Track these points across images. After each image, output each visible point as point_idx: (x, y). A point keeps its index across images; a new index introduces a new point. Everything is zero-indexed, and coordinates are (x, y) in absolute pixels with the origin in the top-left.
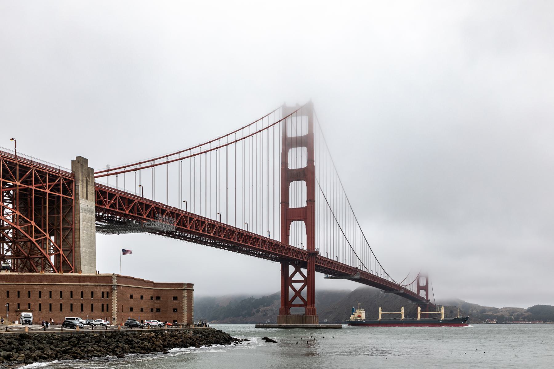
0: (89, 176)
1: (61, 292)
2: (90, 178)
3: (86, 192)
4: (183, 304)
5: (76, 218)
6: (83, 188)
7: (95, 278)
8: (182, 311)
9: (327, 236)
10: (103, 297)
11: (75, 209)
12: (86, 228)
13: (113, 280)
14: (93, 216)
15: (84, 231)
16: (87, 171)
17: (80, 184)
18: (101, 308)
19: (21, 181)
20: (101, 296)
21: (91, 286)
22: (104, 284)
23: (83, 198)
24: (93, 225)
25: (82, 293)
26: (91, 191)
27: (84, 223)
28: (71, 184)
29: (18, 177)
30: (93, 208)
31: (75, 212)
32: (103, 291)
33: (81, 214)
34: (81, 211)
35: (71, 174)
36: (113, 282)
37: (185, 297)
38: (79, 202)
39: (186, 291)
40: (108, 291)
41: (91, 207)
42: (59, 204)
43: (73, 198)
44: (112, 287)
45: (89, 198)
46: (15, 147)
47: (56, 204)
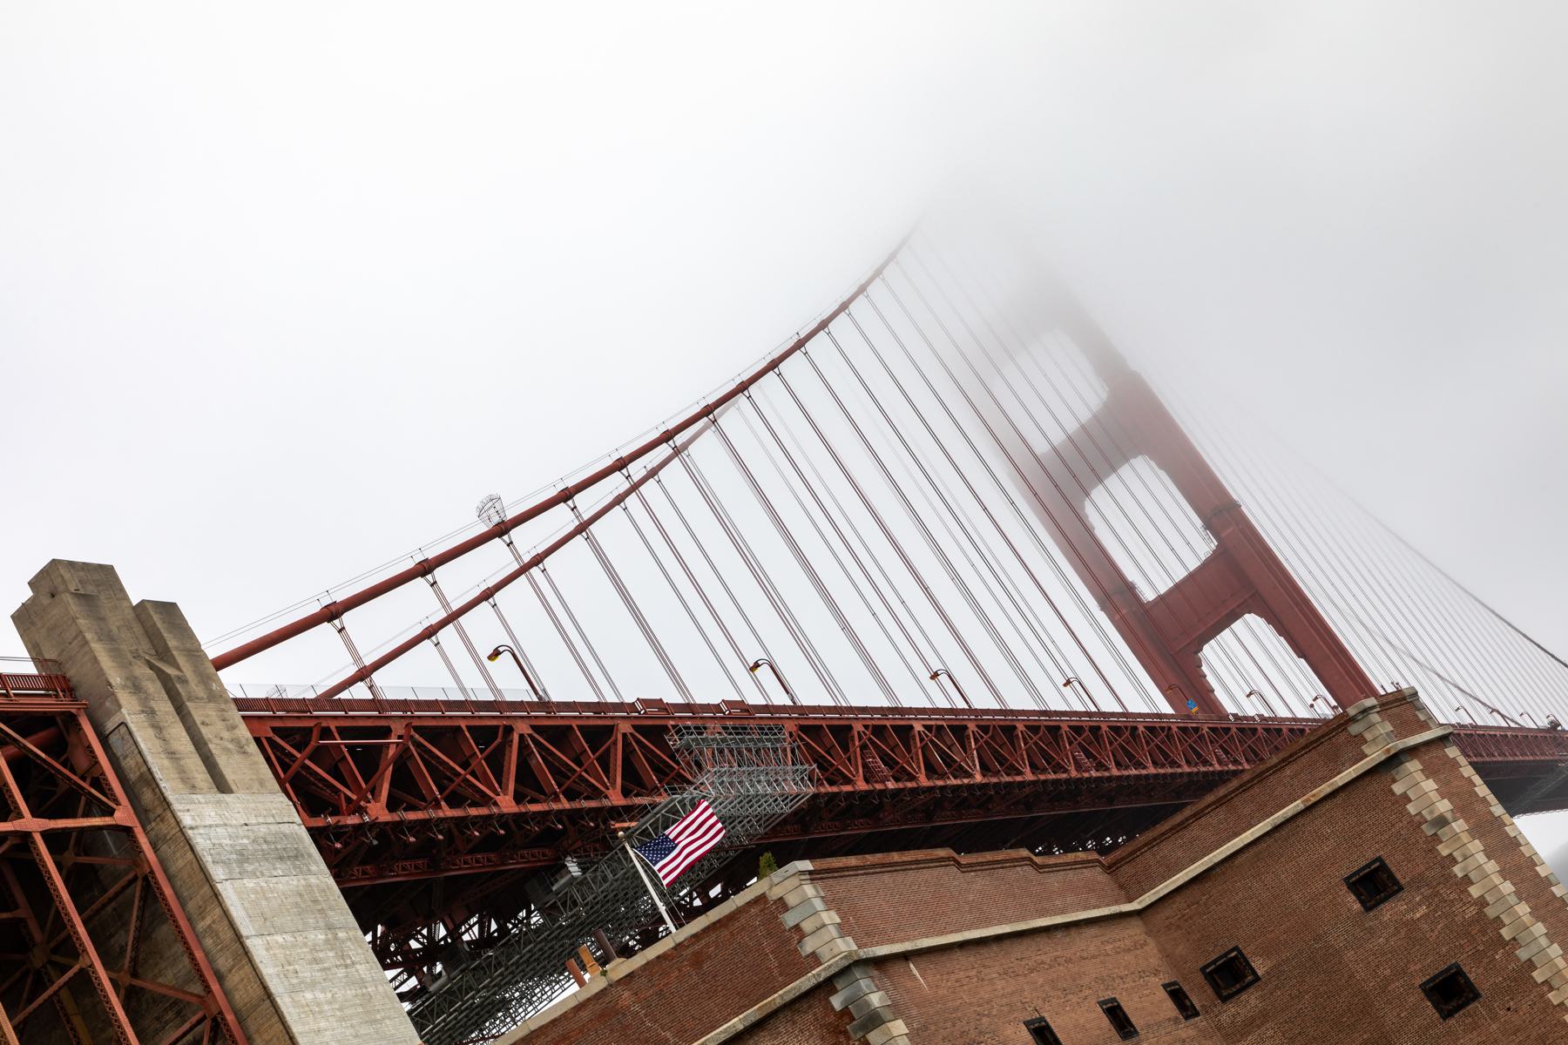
0: (164, 653)
2: (181, 660)
3: (191, 748)
4: (1475, 891)
5: (208, 942)
6: (158, 728)
7: (602, 1016)
8: (1510, 955)
9: (1383, 603)
11: (173, 887)
12: (307, 973)
13: (797, 928)
14: (313, 880)
15: (309, 996)
16: (137, 629)
17: (129, 711)
23: (193, 788)
24: (341, 935)
26: (226, 735)
27: (279, 938)
28: (72, 739)
30: (285, 828)
31: (183, 905)
33: (228, 891)
34: (217, 873)
35: (42, 684)
36: (809, 946)
37: (1442, 822)
38: (178, 823)
39: (1413, 766)
41: (274, 828)
42: (60, 923)
43: (123, 815)
44: (837, 1002)
45: (230, 775)
47: (38, 936)
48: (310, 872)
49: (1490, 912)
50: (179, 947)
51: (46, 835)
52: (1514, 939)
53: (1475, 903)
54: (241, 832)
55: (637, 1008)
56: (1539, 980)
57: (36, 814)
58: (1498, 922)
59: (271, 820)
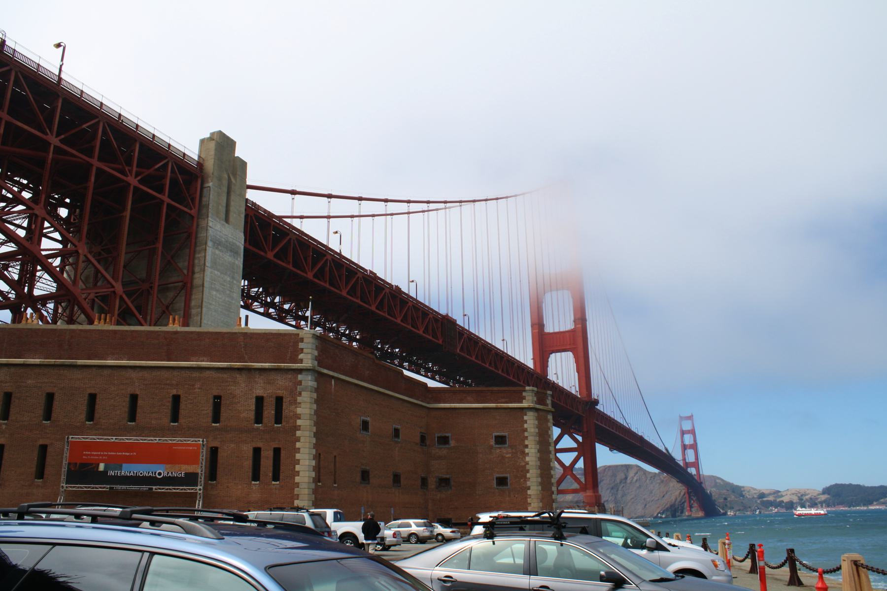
1: (93, 398)
2: (238, 180)
10: (259, 419)
18: (248, 463)
19: (63, 136)
20: (252, 415)
21: (213, 374)
22: (267, 365)
25: (176, 399)
27: (216, 272)
29: (56, 126)
30: (238, 244)
32: (260, 392)
34: (210, 244)
35: (195, 163)
38: (207, 223)
40: (280, 393)
41: (234, 241)
43: (193, 212)
45: (231, 219)
46: (62, 60)
48: (237, 259)
49: (528, 467)
50: (187, 258)
51: (168, 205)
52: (529, 478)
53: (525, 462)
54: (224, 237)
55: (242, 343)
56: (529, 493)
57: (169, 197)
58: (528, 471)
59: (235, 238)
